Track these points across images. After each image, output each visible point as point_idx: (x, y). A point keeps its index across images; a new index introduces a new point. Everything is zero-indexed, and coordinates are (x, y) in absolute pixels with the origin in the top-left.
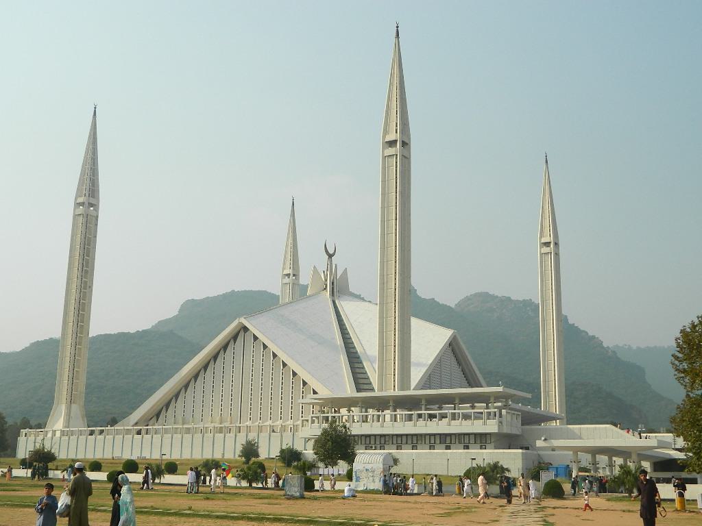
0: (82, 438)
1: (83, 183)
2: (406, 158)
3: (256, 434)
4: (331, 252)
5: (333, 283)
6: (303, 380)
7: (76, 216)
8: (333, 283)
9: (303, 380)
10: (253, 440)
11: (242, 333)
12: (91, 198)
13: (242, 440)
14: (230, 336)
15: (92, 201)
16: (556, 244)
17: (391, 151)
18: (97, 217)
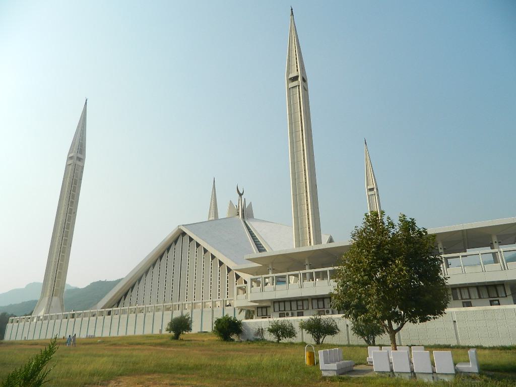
0: (52, 322)
1: (75, 144)
2: (305, 89)
3: (189, 311)
4: (241, 192)
5: (243, 211)
6: (227, 267)
7: (67, 166)
8: (243, 211)
9: (227, 267)
10: (187, 315)
11: (181, 238)
12: (78, 154)
13: (177, 314)
14: (173, 239)
15: (79, 156)
16: (377, 189)
17: (295, 83)
18: (83, 167)
